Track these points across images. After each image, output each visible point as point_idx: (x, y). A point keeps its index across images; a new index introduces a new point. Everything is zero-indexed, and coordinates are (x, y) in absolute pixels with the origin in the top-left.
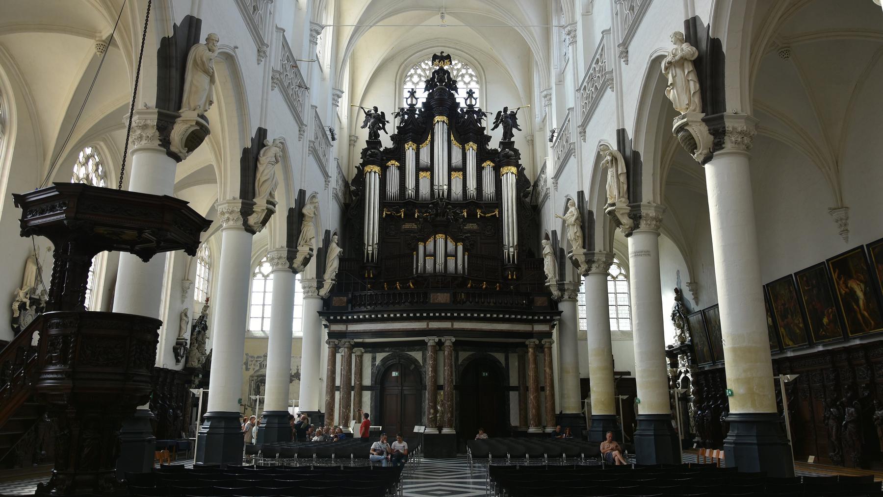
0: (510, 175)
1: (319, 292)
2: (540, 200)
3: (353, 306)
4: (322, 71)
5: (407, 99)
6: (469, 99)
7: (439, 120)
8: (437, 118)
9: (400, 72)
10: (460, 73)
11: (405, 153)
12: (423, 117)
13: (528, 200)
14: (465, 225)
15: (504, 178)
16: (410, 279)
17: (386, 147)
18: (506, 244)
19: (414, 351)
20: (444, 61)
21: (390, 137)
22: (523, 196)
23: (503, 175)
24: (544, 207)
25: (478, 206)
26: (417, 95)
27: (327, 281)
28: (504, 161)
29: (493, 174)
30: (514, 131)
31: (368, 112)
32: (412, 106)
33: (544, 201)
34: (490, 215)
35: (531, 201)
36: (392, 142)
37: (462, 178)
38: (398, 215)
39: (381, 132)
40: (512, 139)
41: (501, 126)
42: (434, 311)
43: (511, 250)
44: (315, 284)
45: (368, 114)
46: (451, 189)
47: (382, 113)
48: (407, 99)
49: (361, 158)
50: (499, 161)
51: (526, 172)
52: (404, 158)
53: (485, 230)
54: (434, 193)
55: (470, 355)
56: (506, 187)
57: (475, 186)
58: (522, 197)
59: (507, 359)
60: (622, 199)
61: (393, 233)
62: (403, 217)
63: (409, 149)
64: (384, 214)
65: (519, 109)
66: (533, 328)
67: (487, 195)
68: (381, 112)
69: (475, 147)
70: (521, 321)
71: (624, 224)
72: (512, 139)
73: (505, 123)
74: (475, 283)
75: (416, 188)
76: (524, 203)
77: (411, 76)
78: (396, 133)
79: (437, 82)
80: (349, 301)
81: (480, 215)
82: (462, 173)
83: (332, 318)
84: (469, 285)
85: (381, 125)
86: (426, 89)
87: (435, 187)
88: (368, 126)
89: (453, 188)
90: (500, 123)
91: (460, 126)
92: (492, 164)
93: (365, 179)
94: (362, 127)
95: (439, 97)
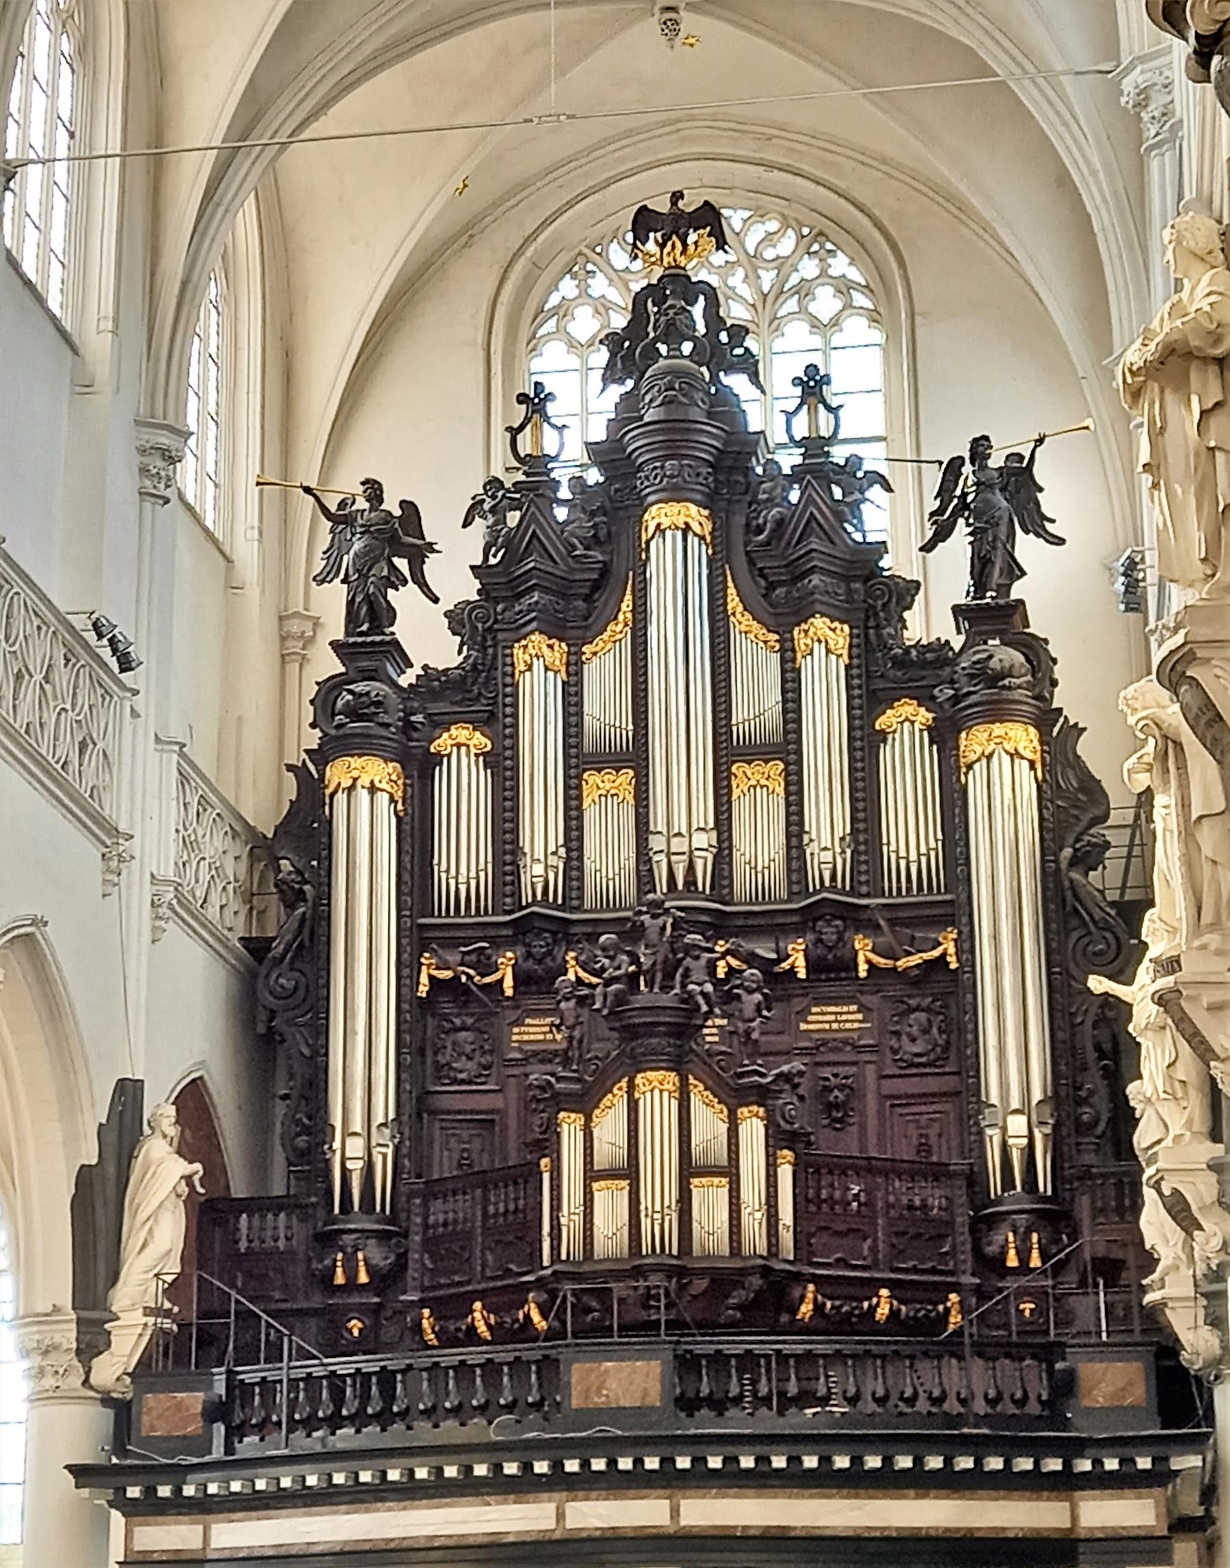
1: (88, 1373)
3: (235, 1433)
4: (75, 351)
7: (666, 523)
10: (794, 279)
11: (515, 686)
12: (593, 514)
17: (425, 667)
18: (994, 1099)
21: (445, 614)
23: (970, 767)
27: (126, 1318)
28: (973, 699)
29: (930, 756)
30: (1027, 547)
31: (342, 505)
32: (537, 464)
36: (458, 639)
37: (780, 790)
38: (488, 980)
39: (404, 599)
40: (1018, 591)
41: (961, 537)
42: (585, 1449)
44: (68, 1336)
45: (342, 519)
46: (730, 847)
47: (409, 507)
49: (313, 725)
51: (1083, 748)
53: (897, 1034)
54: (651, 870)
56: (983, 825)
57: (843, 826)
58: (1064, 865)
60: (1206, 938)
61: (470, 1065)
62: (509, 992)
63: (530, 668)
64: (424, 979)
65: (1040, 441)
66: (1074, 1518)
67: (903, 863)
68: (402, 503)
69: (840, 637)
70: (1007, 1483)
71: (1222, 1056)
72: (1018, 591)
74: (831, 1298)
75: (569, 851)
76: (1076, 896)
77: (563, 311)
79: (656, 340)
80: (215, 1412)
81: (868, 961)
82: (782, 766)
83: (134, 1492)
85: (402, 564)
86: (610, 375)
87: (657, 843)
88: (342, 576)
92: (924, 716)
93: (330, 822)
94: (321, 580)
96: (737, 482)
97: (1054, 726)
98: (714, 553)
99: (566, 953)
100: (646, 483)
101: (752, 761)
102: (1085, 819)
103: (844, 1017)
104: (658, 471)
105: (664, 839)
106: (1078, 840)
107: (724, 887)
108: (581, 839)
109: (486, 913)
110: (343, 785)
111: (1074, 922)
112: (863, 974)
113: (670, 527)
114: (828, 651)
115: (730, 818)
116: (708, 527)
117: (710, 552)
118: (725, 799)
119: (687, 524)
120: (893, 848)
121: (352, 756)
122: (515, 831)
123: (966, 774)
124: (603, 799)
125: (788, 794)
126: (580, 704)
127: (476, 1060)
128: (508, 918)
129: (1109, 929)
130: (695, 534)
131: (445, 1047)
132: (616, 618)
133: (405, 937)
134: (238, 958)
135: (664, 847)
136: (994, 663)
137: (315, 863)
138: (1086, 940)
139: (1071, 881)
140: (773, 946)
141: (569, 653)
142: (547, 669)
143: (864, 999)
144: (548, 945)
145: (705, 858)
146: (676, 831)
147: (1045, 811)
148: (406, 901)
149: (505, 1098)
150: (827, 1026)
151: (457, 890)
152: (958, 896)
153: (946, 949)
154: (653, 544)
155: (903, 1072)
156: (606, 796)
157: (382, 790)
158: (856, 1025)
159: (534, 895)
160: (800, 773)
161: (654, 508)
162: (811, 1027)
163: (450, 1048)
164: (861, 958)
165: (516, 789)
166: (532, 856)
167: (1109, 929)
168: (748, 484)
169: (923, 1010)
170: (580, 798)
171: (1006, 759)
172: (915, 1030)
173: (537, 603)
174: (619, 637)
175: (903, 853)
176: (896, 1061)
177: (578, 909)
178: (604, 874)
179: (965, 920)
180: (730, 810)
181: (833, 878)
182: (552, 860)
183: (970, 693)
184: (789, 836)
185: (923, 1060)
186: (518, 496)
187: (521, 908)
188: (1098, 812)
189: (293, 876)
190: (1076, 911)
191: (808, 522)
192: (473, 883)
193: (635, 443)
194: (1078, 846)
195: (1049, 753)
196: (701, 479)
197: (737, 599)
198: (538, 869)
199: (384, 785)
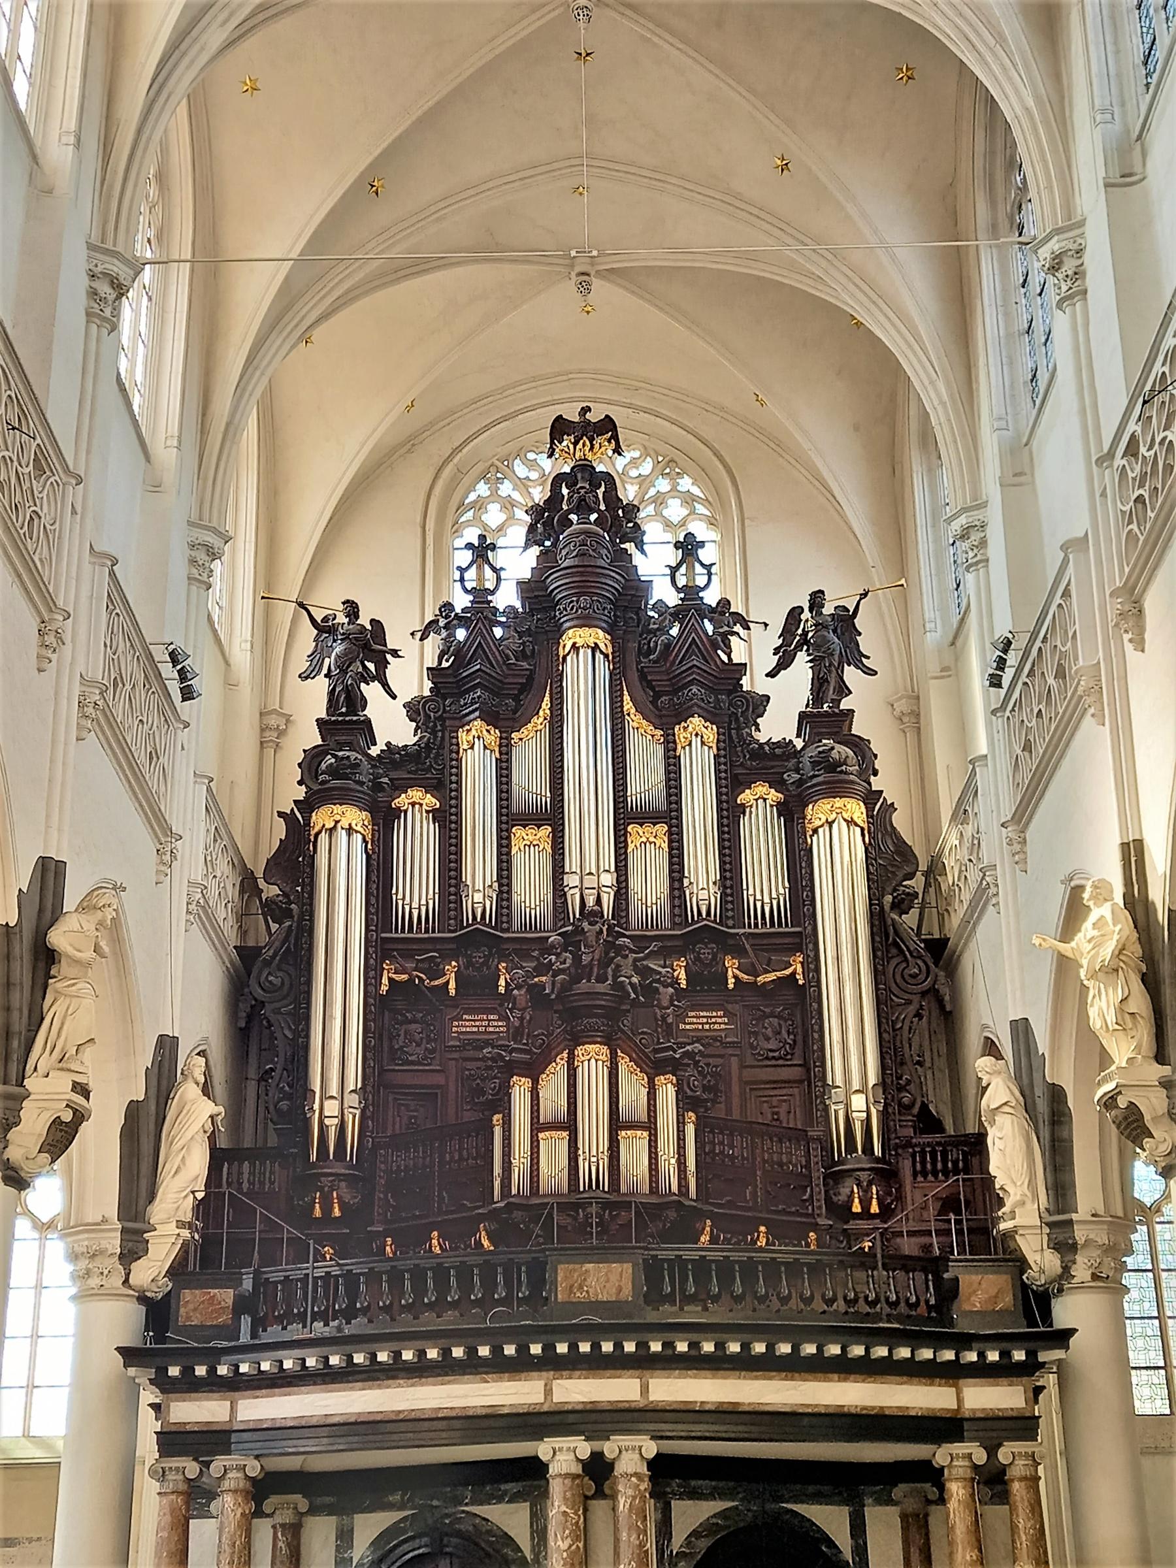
0: (840, 828)
2: (955, 921)
5: (462, 570)
6: (683, 570)
7: (580, 642)
8: (568, 640)
9: (440, 484)
13: (910, 919)
14: (681, 1017)
15: (819, 845)
16: (481, 1218)
19: (500, 1500)
20: (591, 440)
22: (894, 906)
23: (815, 831)
24: (972, 945)
25: (728, 944)
26: (499, 558)
28: (820, 779)
32: (481, 595)
33: (971, 922)
34: (772, 976)
35: (919, 927)
37: (665, 846)
38: (436, 983)
43: (858, 1102)
46: (627, 887)
48: (462, 570)
50: (800, 783)
52: (454, 778)
55: (714, 1516)
57: (714, 875)
58: (887, 907)
59: (858, 1528)
62: (452, 992)
64: (385, 980)
67: (759, 904)
73: (817, 647)
75: (500, 885)
78: (427, 693)
81: (735, 977)
84: (705, 1238)
87: (572, 880)
89: (635, 883)
90: (799, 647)
91: (655, 662)
95: (576, 562)
96: (631, 618)
97: (876, 804)
98: (614, 669)
99: (499, 963)
100: (565, 613)
101: (644, 823)
102: (900, 875)
103: (713, 1020)
104: (575, 603)
105: (577, 878)
106: (895, 890)
107: (622, 918)
108: (509, 877)
109: (433, 932)
110: (327, 826)
111: (894, 951)
112: (731, 986)
113: (583, 646)
114: (703, 743)
115: (626, 866)
116: (610, 650)
117: (611, 667)
118: (623, 851)
119: (596, 644)
120: (751, 891)
121: (335, 804)
122: (459, 870)
123: (811, 836)
124: (527, 848)
125: (671, 848)
126: (509, 776)
127: (423, 1046)
128: (453, 935)
129: (920, 957)
130: (602, 652)
131: (399, 1036)
132: (538, 713)
133: (372, 947)
134: (232, 962)
135: (577, 883)
136: (834, 754)
137: (299, 889)
138: (904, 965)
139: (893, 920)
140: (662, 962)
141: (501, 738)
142: (485, 748)
143: (729, 1007)
144: (485, 956)
145: (609, 893)
146: (588, 871)
147: (871, 867)
148: (373, 919)
149: (447, 1079)
150: (700, 1027)
151: (411, 913)
152: (805, 928)
153: (795, 969)
154: (569, 658)
155: (760, 1063)
156: (529, 846)
157: (357, 832)
158: (723, 1026)
159: (474, 918)
160: (680, 834)
161: (571, 631)
162: (688, 1027)
163: (402, 1037)
164: (730, 973)
165: (459, 838)
166: (474, 887)
167: (920, 957)
168: (639, 620)
169: (776, 1017)
170: (509, 846)
171: (844, 824)
172: (769, 1032)
173: (479, 697)
174: (539, 727)
175: (759, 897)
176: (754, 1054)
177: (507, 930)
178: (528, 905)
179: (811, 946)
180: (626, 859)
181: (708, 913)
182: (489, 892)
183: (815, 776)
184: (672, 880)
185: (776, 1054)
186: (469, 615)
187: (463, 928)
188: (908, 869)
189: (280, 898)
190: (895, 942)
191: (690, 645)
192: (423, 909)
193: (555, 583)
194: (895, 894)
195: (873, 824)
196: (606, 612)
197: (631, 704)
198: (478, 897)
199: (359, 828)
